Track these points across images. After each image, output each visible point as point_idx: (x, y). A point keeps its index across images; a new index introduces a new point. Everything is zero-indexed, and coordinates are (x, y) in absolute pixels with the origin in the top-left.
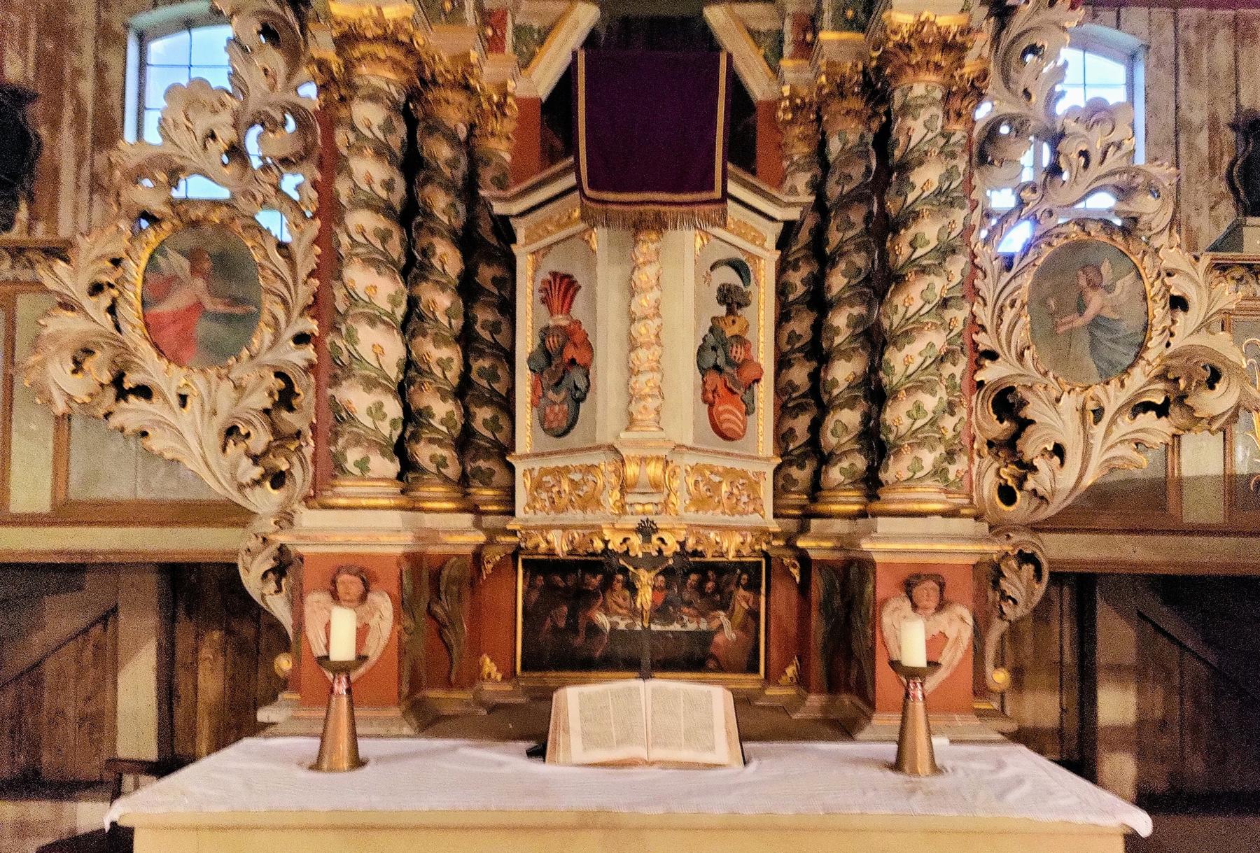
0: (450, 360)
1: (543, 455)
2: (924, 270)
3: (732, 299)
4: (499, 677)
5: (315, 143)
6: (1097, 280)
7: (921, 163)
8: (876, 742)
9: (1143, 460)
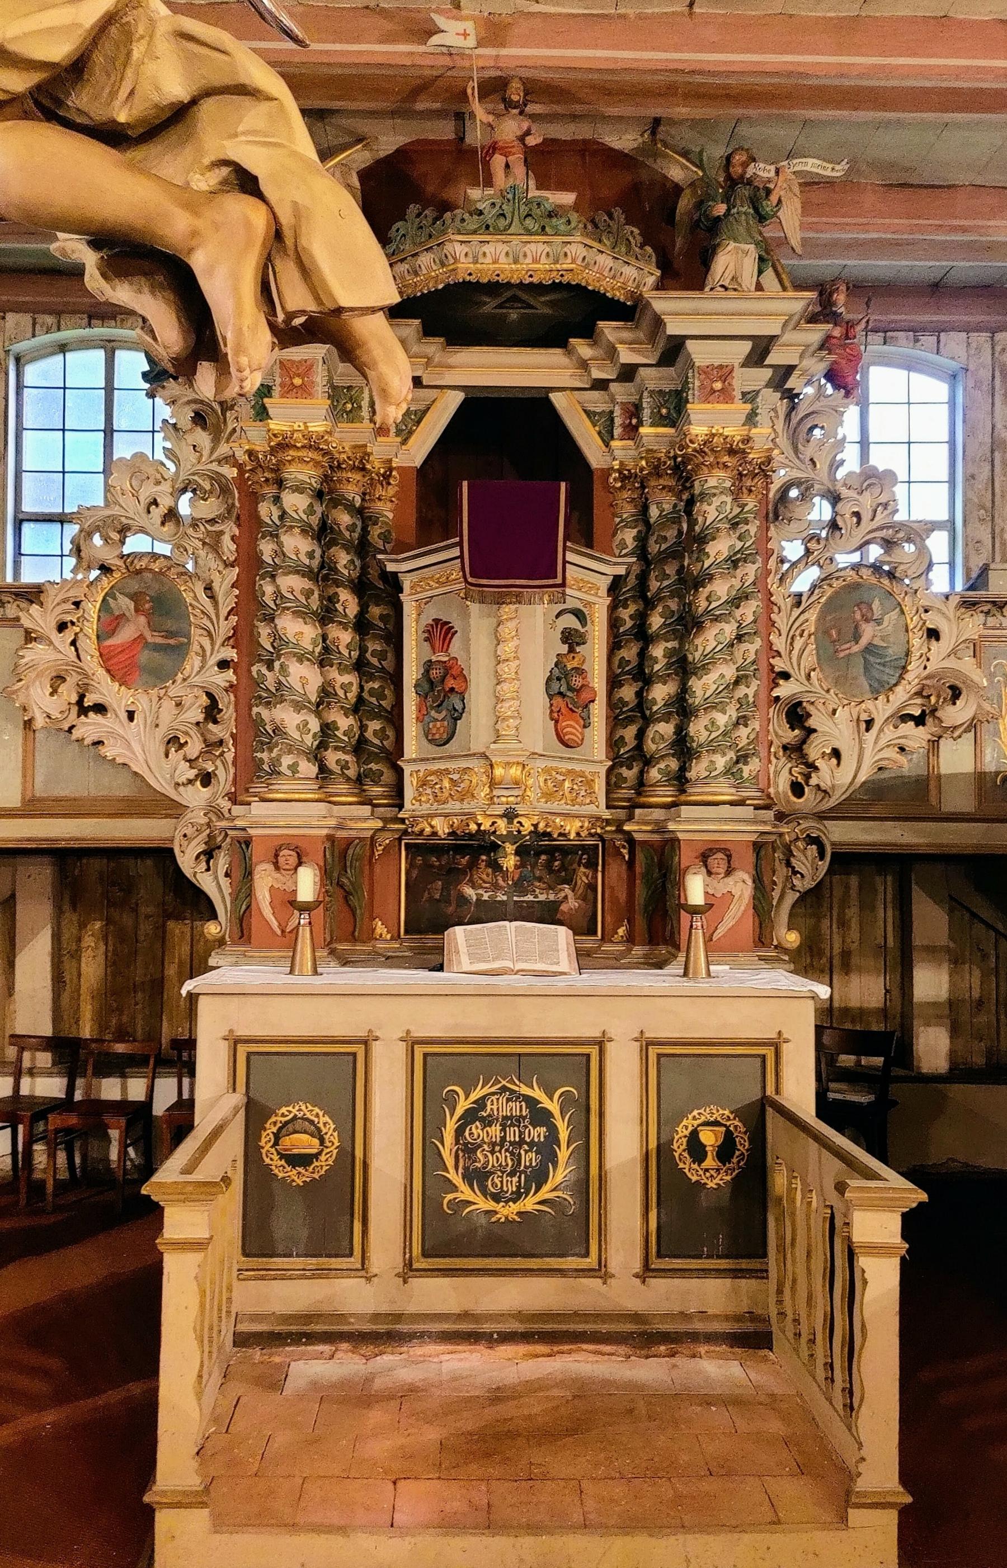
0: (351, 684)
1: (428, 760)
2: (717, 619)
3: (572, 639)
4: (389, 937)
5: (233, 504)
6: (869, 615)
7: (714, 539)
8: (676, 968)
9: (902, 759)
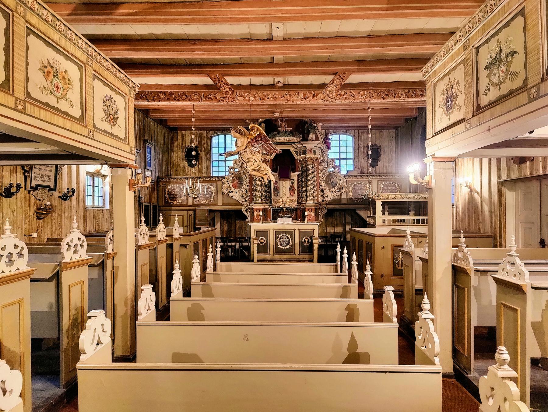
3: (292, 183)
